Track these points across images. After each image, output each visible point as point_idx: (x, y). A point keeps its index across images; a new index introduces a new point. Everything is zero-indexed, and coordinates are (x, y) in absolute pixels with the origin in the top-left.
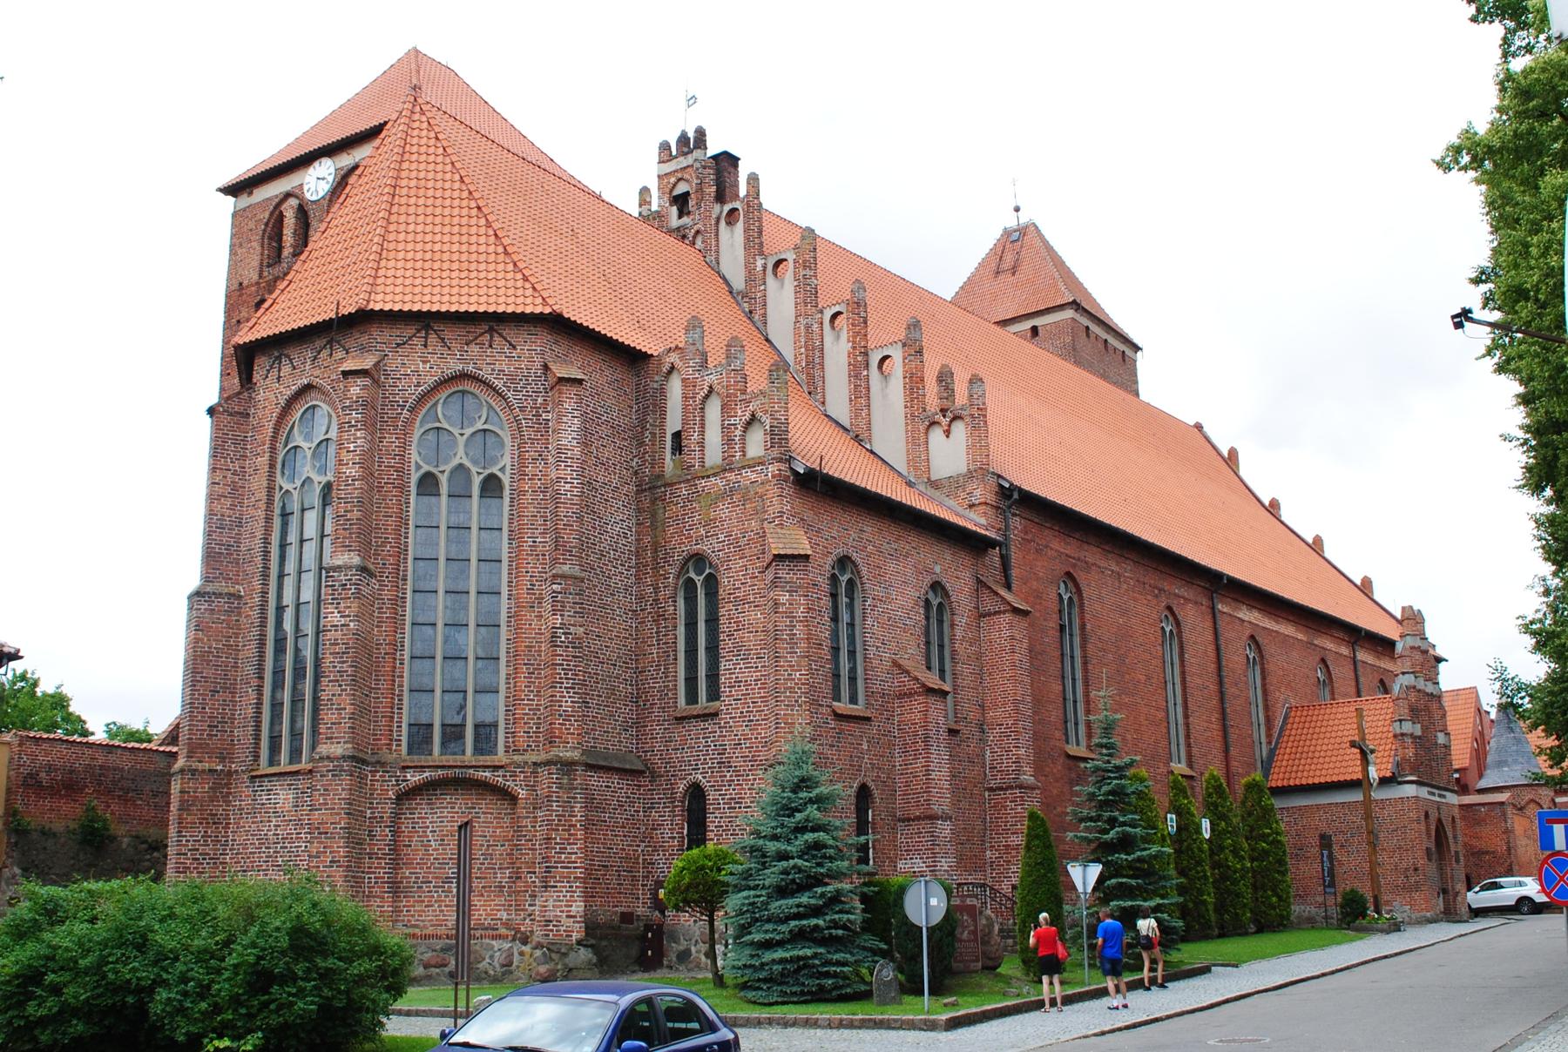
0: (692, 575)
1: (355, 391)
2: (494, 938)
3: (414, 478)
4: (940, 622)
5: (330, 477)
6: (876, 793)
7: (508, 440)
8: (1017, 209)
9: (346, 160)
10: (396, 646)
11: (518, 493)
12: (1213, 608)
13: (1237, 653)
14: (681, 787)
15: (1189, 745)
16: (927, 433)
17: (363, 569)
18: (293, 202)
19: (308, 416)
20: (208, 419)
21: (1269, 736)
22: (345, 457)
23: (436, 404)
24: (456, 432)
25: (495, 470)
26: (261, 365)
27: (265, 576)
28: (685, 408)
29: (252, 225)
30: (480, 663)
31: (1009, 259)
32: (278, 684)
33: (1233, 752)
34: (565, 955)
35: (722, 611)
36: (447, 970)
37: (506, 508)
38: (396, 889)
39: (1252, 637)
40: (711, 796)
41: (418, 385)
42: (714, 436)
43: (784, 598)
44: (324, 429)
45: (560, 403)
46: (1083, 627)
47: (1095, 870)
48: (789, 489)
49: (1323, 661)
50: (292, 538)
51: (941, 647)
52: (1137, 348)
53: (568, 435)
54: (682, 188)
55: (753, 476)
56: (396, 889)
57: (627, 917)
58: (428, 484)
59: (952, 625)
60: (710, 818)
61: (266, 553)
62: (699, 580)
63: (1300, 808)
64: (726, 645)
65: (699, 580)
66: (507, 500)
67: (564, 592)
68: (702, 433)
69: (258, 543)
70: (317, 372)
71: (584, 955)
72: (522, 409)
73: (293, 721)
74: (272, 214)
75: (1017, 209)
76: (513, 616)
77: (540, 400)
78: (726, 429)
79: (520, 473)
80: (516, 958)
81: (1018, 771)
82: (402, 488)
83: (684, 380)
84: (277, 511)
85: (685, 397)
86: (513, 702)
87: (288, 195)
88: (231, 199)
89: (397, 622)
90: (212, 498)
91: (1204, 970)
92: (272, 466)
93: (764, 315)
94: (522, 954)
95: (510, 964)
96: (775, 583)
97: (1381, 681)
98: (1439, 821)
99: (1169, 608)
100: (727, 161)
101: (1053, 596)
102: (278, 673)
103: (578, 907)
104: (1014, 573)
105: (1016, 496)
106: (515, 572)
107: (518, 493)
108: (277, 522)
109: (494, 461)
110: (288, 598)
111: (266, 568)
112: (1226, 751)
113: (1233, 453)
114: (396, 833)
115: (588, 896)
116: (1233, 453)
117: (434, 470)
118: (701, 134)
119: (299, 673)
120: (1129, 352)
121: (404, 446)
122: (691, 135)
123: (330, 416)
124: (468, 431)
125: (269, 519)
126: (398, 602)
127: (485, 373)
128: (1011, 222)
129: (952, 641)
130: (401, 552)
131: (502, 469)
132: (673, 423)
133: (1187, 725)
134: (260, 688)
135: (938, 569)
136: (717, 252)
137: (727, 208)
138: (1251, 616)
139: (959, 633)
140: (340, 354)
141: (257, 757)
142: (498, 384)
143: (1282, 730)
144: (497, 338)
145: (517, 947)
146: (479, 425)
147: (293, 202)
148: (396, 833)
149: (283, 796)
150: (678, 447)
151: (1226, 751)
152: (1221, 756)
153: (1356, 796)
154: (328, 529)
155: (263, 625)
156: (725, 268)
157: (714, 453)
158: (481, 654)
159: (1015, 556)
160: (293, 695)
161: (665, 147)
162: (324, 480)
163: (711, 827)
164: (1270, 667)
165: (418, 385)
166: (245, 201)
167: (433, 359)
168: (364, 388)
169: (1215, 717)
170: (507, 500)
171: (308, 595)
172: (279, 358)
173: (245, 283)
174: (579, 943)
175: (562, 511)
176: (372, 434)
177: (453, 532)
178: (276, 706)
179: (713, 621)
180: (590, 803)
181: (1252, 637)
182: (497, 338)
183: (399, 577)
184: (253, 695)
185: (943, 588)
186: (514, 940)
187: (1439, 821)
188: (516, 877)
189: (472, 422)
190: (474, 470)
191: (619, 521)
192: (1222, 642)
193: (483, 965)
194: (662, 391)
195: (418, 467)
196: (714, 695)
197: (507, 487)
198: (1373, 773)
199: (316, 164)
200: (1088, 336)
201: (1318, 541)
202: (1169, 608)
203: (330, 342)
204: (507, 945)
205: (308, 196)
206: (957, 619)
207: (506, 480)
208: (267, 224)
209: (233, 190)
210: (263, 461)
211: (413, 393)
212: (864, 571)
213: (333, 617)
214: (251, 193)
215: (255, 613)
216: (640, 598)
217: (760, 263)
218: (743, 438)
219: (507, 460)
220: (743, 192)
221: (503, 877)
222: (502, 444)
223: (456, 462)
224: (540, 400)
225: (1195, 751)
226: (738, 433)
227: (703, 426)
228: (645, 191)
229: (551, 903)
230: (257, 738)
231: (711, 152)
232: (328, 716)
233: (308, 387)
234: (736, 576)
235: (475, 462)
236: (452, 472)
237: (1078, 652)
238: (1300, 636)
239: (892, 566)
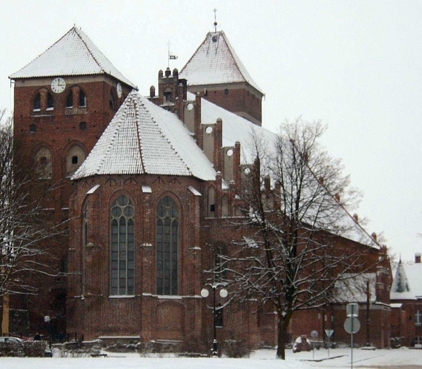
5: (131, 217)
8: (216, 24)
9: (71, 82)
29: (25, 94)
41: (158, 194)
45: (195, 202)
52: (262, 95)
54: (168, 90)
69: (106, 234)
72: (183, 202)
75: (216, 24)
127: (174, 191)
128: (212, 29)
140: (134, 183)
142: (177, 194)
144: (176, 181)
161: (160, 74)
162: (129, 218)
165: (158, 194)
166: (20, 84)
167: (161, 187)
168: (150, 197)
173: (24, 116)
182: (176, 181)
195: (157, 217)
199: (57, 79)
200: (248, 95)
221: (179, 326)
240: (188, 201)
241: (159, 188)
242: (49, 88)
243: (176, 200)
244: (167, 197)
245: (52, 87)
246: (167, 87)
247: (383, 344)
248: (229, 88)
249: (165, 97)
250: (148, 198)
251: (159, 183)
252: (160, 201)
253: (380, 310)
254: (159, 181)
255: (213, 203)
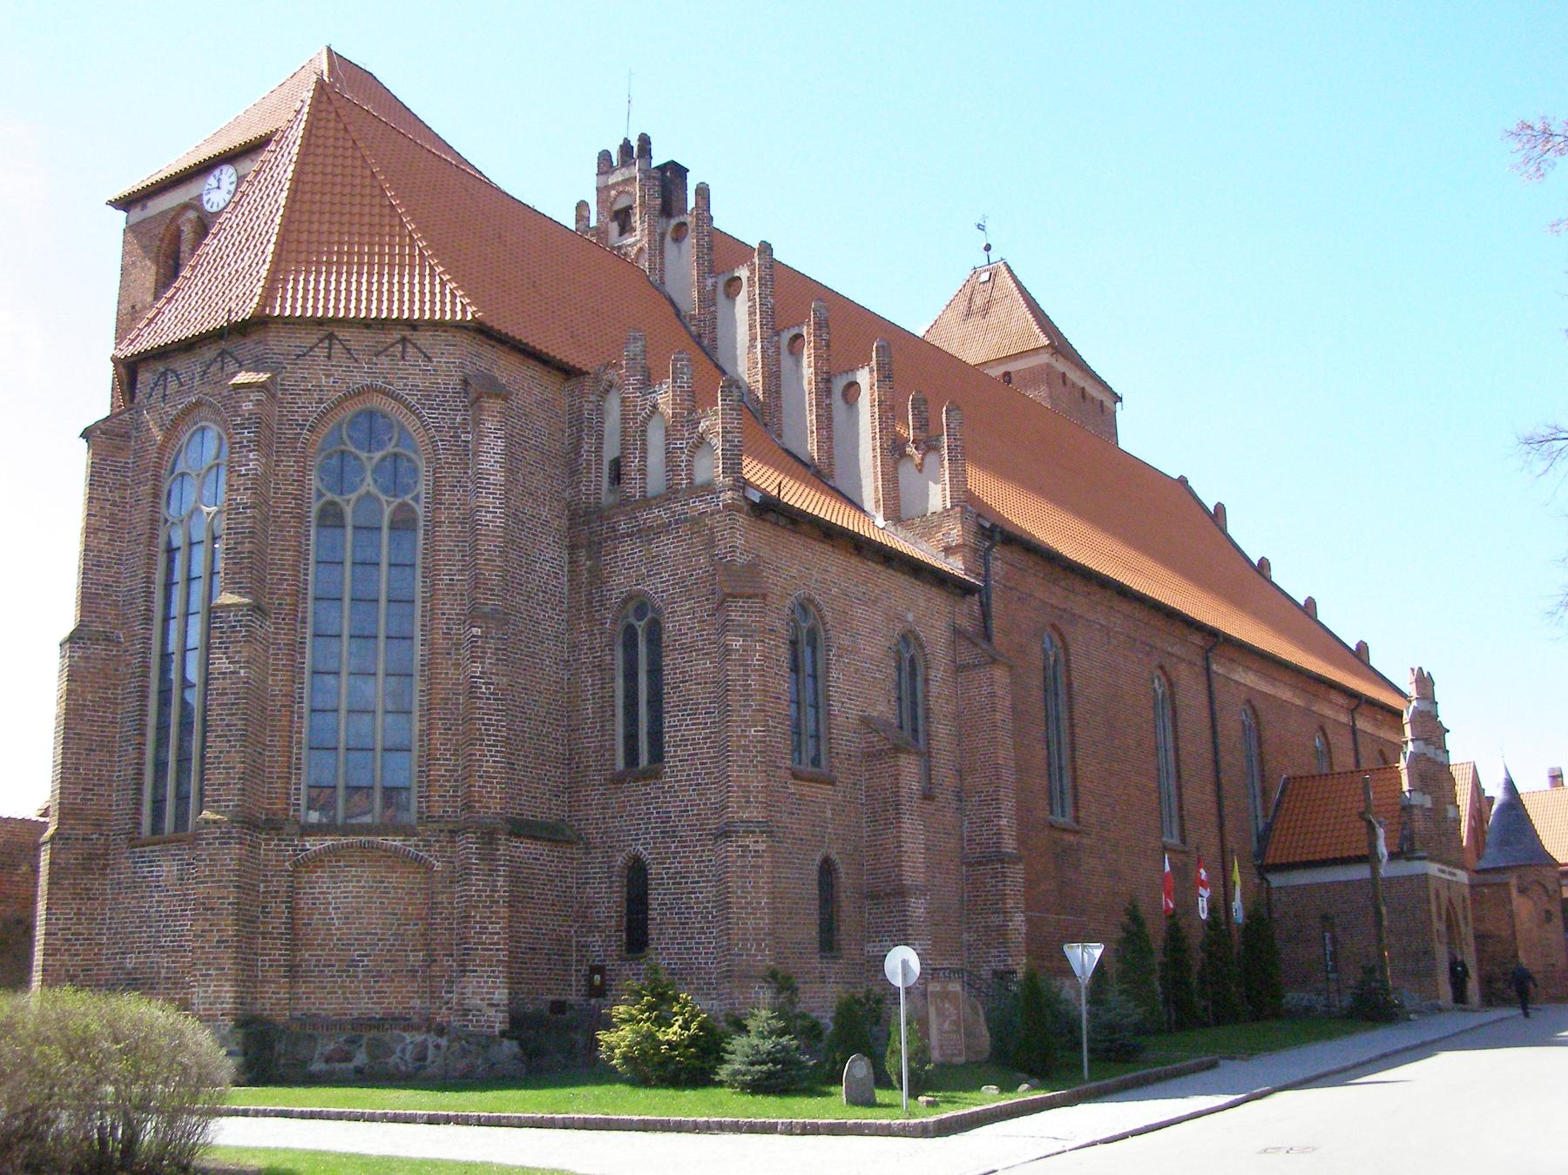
0: (632, 620)
1: (247, 406)
2: (405, 1029)
3: (315, 508)
4: (913, 675)
6: (842, 869)
7: (422, 465)
8: (988, 248)
10: (292, 699)
11: (434, 524)
12: (1208, 670)
13: (1231, 724)
14: (620, 860)
15: (1181, 817)
16: (896, 469)
17: (257, 608)
18: (192, 215)
19: (198, 438)
20: (83, 443)
21: (1265, 809)
22: (236, 482)
23: (340, 426)
24: (364, 455)
25: (408, 498)
26: (145, 377)
27: (148, 620)
28: (624, 432)
30: (390, 718)
31: (979, 301)
32: (162, 741)
33: (1228, 825)
34: (486, 1047)
35: (667, 660)
36: (351, 1065)
37: (421, 542)
38: (293, 972)
39: (1249, 701)
40: (653, 870)
41: (321, 401)
42: (656, 458)
43: (737, 643)
44: (214, 452)
45: (478, 422)
46: (1069, 685)
47: (1097, 951)
48: (741, 519)
49: (1322, 728)
50: (179, 575)
51: (914, 704)
53: (491, 459)
54: (621, 204)
55: (701, 507)
56: (293, 972)
57: (559, 1007)
58: (331, 517)
59: (926, 681)
60: (652, 894)
61: (149, 594)
62: (641, 626)
63: (1298, 887)
64: (670, 699)
65: (641, 626)
66: (421, 533)
67: (485, 636)
68: (644, 458)
69: (139, 584)
70: (207, 389)
71: (510, 1047)
72: (438, 429)
73: (179, 784)
74: (167, 229)
76: (429, 664)
77: (458, 419)
78: (669, 454)
79: (436, 500)
80: (431, 1051)
81: (998, 844)
82: (302, 518)
83: (623, 400)
84: (162, 547)
85: (624, 419)
86: (428, 759)
87: (186, 207)
88: (122, 215)
89: (295, 671)
90: (90, 531)
91: (1212, 1065)
92: (156, 496)
93: (714, 340)
94: (437, 1047)
95: (424, 1058)
96: (724, 629)
97: (1381, 753)
98: (1450, 900)
99: (1161, 667)
100: (675, 172)
101: (1037, 649)
102: (163, 728)
103: (501, 995)
104: (995, 624)
105: (998, 537)
106: (431, 614)
107: (434, 524)
108: (162, 559)
109: (406, 489)
110: (173, 646)
111: (149, 610)
112: (1221, 826)
113: (1220, 508)
114: (293, 910)
115: (513, 982)
116: (1220, 508)
117: (337, 499)
118: (645, 141)
119: (186, 725)
120: (1108, 403)
121: (303, 471)
122: (635, 143)
123: (220, 438)
124: (378, 455)
125: (151, 557)
126: (296, 648)
129: (926, 696)
130: (299, 594)
131: (416, 499)
132: (611, 450)
133: (1180, 796)
134: (140, 748)
135: (910, 617)
136: (661, 270)
137: (674, 222)
138: (1248, 678)
139: (934, 688)
140: (232, 367)
141: (138, 825)
142: (412, 400)
143: (1279, 803)
145: (432, 1039)
146: (390, 448)
147: (192, 215)
148: (293, 910)
149: (167, 869)
150: (617, 475)
151: (1221, 826)
152: (1216, 831)
153: (1361, 872)
154: (220, 565)
155: (145, 675)
156: (672, 288)
157: (656, 480)
158: (390, 707)
159: (997, 606)
160: (179, 756)
161: (605, 157)
163: (654, 904)
164: (1267, 735)
165: (321, 401)
166: (138, 214)
169: (1209, 788)
170: (421, 533)
171: (195, 638)
172: (164, 374)
174: (503, 1034)
175: (483, 545)
176: (267, 456)
177: (359, 569)
178: (160, 766)
179: (655, 671)
180: (515, 877)
181: (1249, 701)
182: (410, 349)
183: (297, 619)
184: (132, 753)
185: (917, 638)
186: (428, 1031)
187: (1450, 900)
188: (431, 960)
189: (381, 445)
190: (383, 498)
191: (550, 557)
192: (1217, 707)
193: (394, 1059)
194: (600, 410)
195: (320, 495)
196: (657, 755)
197: (421, 523)
198: (1383, 850)
200: (1064, 382)
201: (1311, 603)
202: (1161, 667)
203: (222, 354)
204: (419, 1038)
205: (207, 207)
206: (932, 673)
207: (420, 510)
208: (162, 240)
209: (125, 203)
210: (146, 489)
211: (314, 410)
212: (829, 617)
213: (221, 663)
214: (144, 207)
215: (137, 660)
216: (574, 647)
217: (710, 282)
218: (690, 464)
219: (422, 488)
220: (691, 203)
221: (416, 958)
222: (415, 470)
223: (362, 490)
224: (458, 419)
225: (1188, 824)
226: (684, 457)
227: (644, 451)
228: (582, 206)
229: (470, 990)
230: (138, 803)
231: (655, 163)
232: (216, 776)
233: (199, 404)
234: (683, 621)
235: (386, 492)
236: (358, 500)
237: (1064, 715)
238: (1298, 702)
239: (859, 612)
240: (465, 422)
241: (327, 376)
242: (195, 204)
243: (411, 424)
244: (371, 414)
245: (205, 198)
246: (620, 193)
247: (1445, 991)
248: (1011, 367)
249: (614, 227)
250: (250, 406)
251: (329, 357)
252: (340, 426)
253: (1426, 875)
254: (330, 348)
255: (617, 454)
